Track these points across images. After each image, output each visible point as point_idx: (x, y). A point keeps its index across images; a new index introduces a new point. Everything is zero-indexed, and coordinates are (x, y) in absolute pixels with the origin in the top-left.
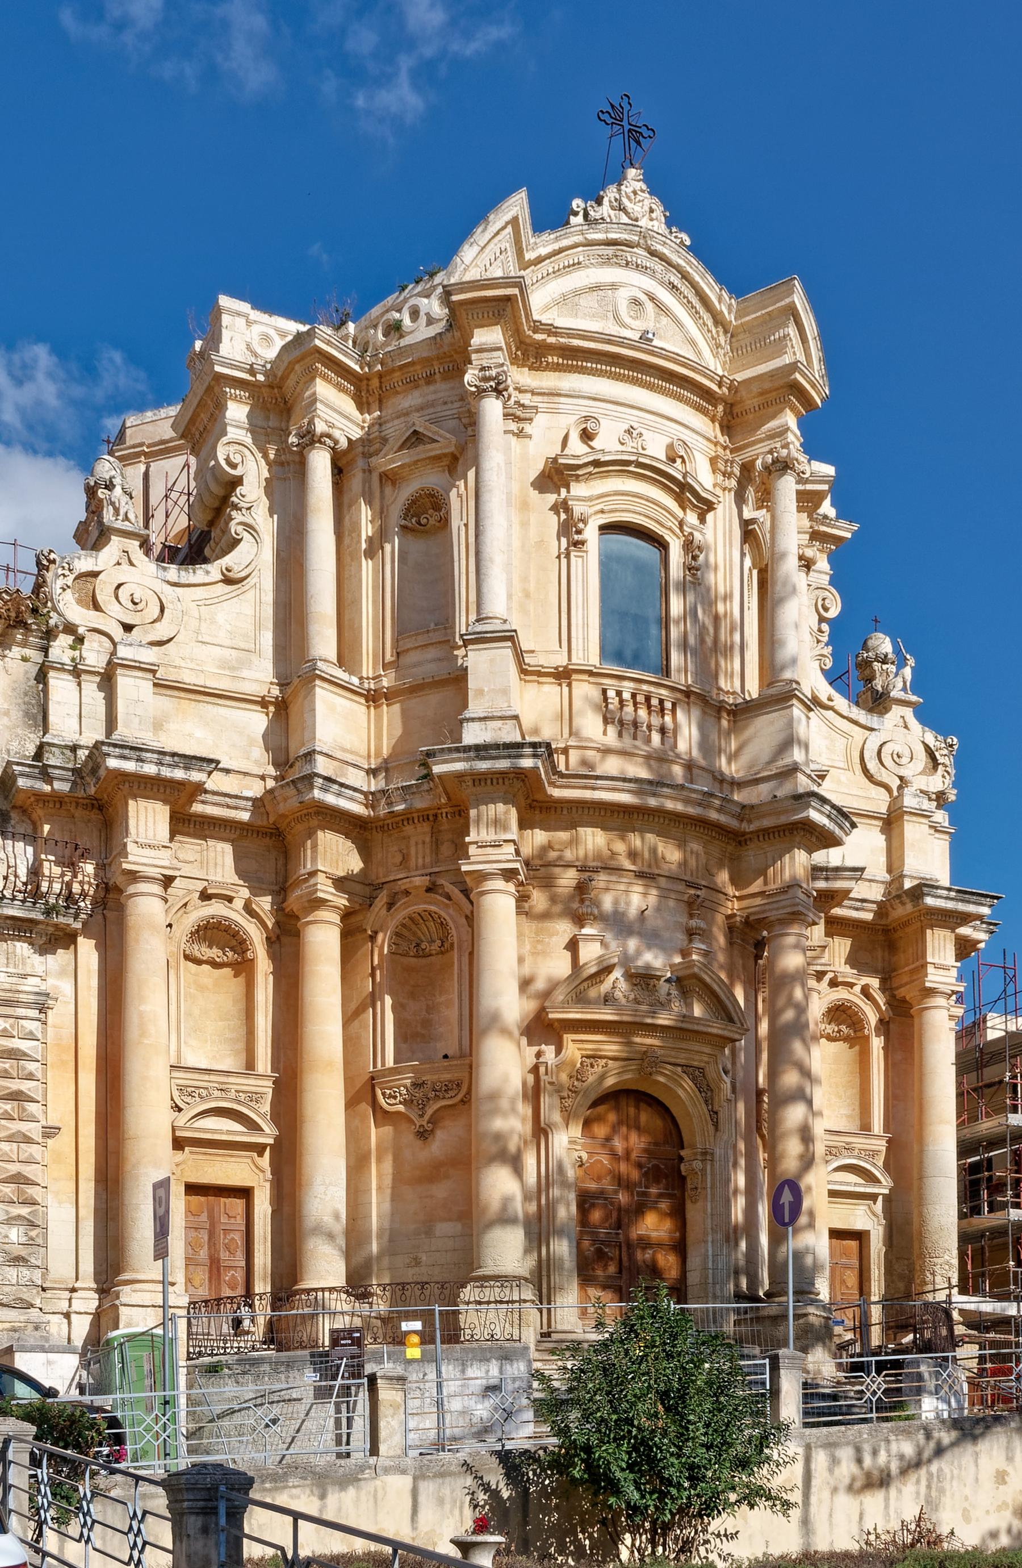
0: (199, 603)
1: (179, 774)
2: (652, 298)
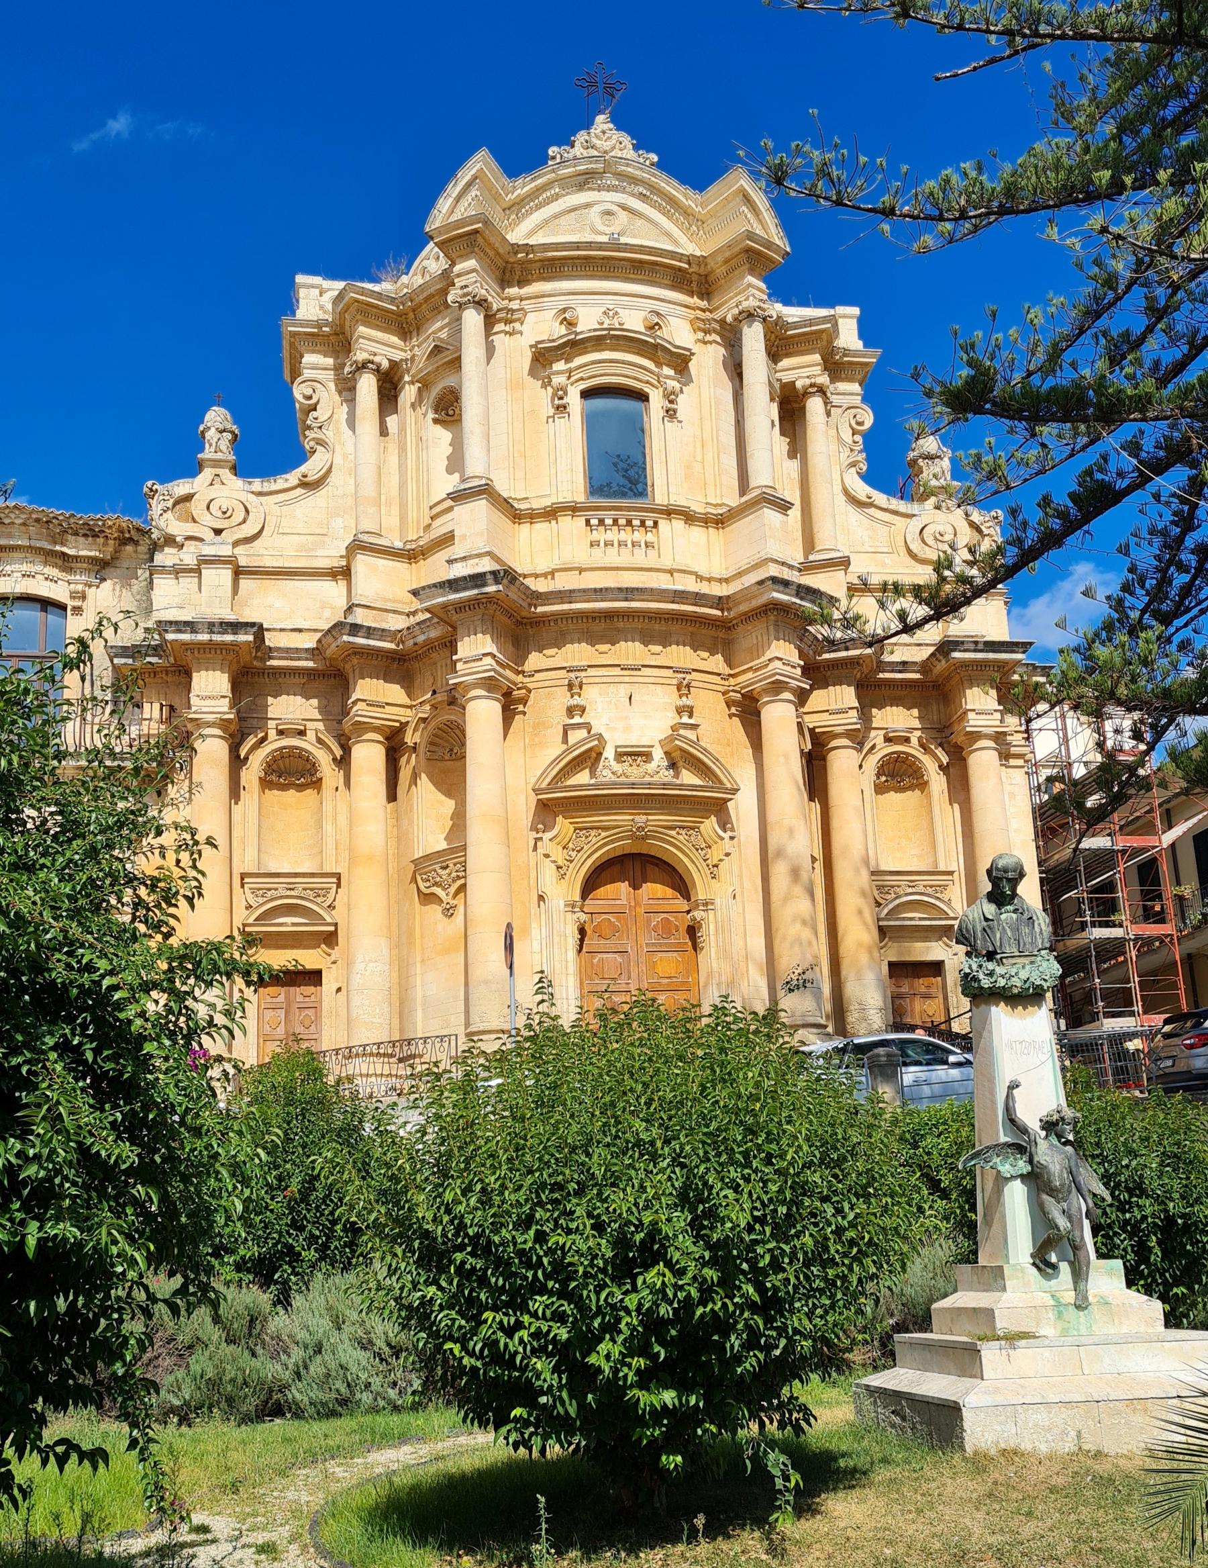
0: (280, 504)
1: (229, 638)
2: (624, 207)
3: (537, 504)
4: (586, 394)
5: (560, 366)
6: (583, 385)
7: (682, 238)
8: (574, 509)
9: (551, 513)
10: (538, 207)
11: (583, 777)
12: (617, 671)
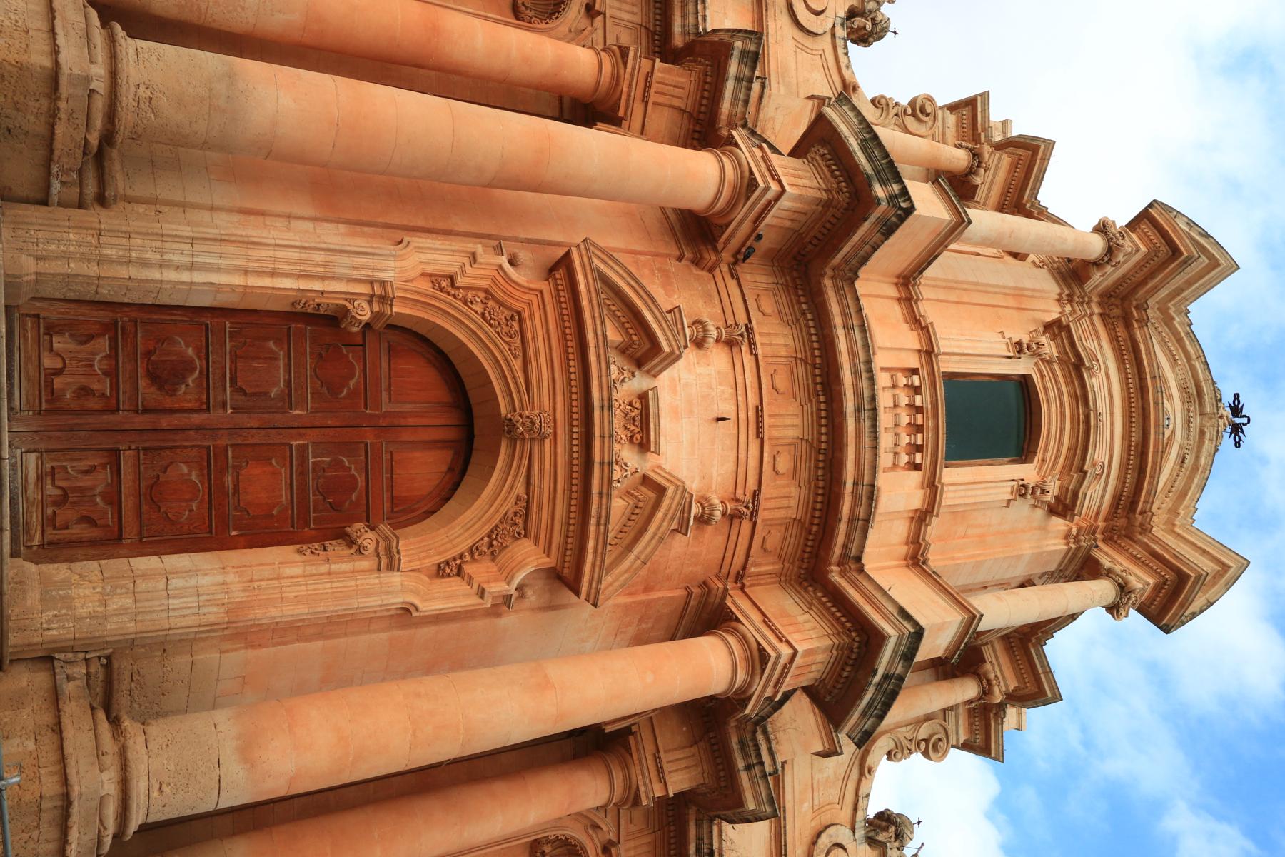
0: (822, 55)
8: (929, 353)
12: (753, 400)
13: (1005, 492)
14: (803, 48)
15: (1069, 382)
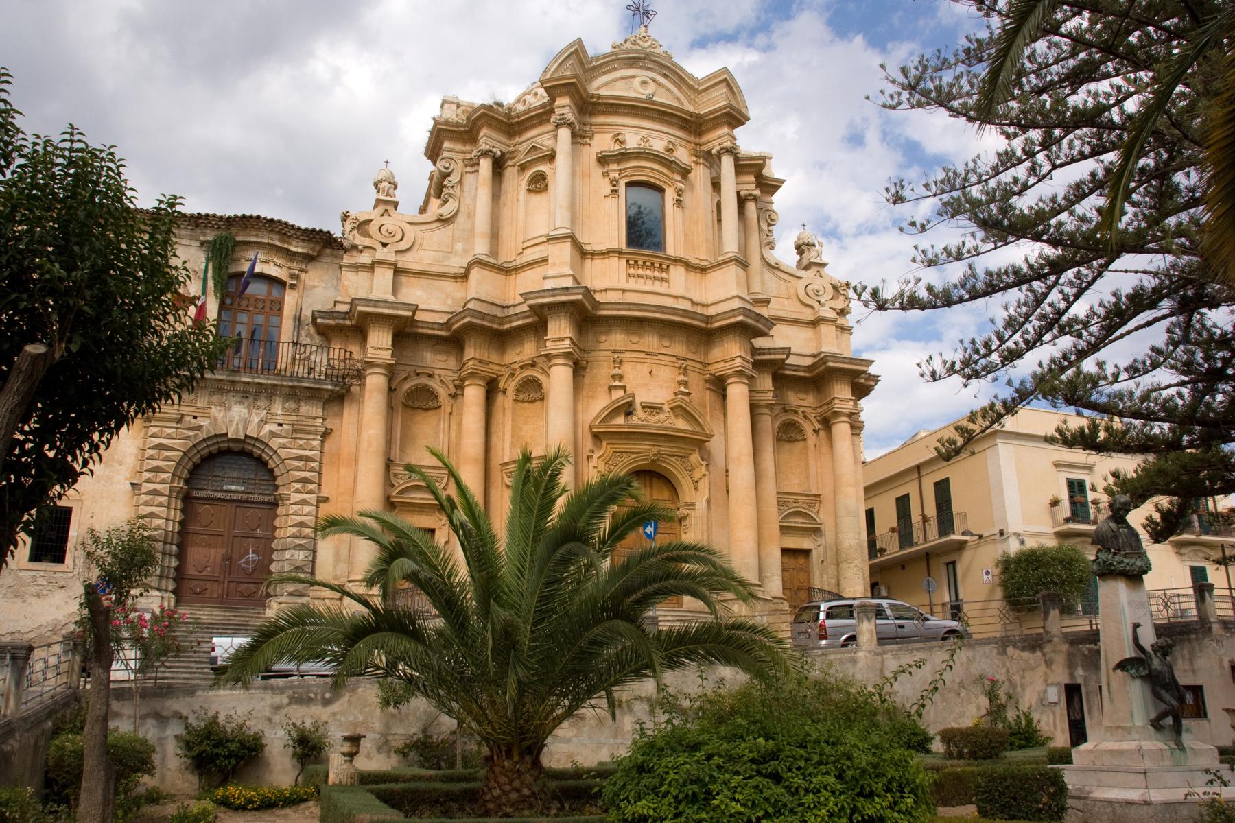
2: (654, 81)
3: (598, 248)
4: (628, 185)
5: (614, 167)
6: (627, 180)
7: (686, 103)
8: (620, 253)
9: (606, 254)
10: (605, 73)
11: (620, 420)
12: (643, 355)
13: (678, 211)
14: (421, 244)
15: (629, 160)
